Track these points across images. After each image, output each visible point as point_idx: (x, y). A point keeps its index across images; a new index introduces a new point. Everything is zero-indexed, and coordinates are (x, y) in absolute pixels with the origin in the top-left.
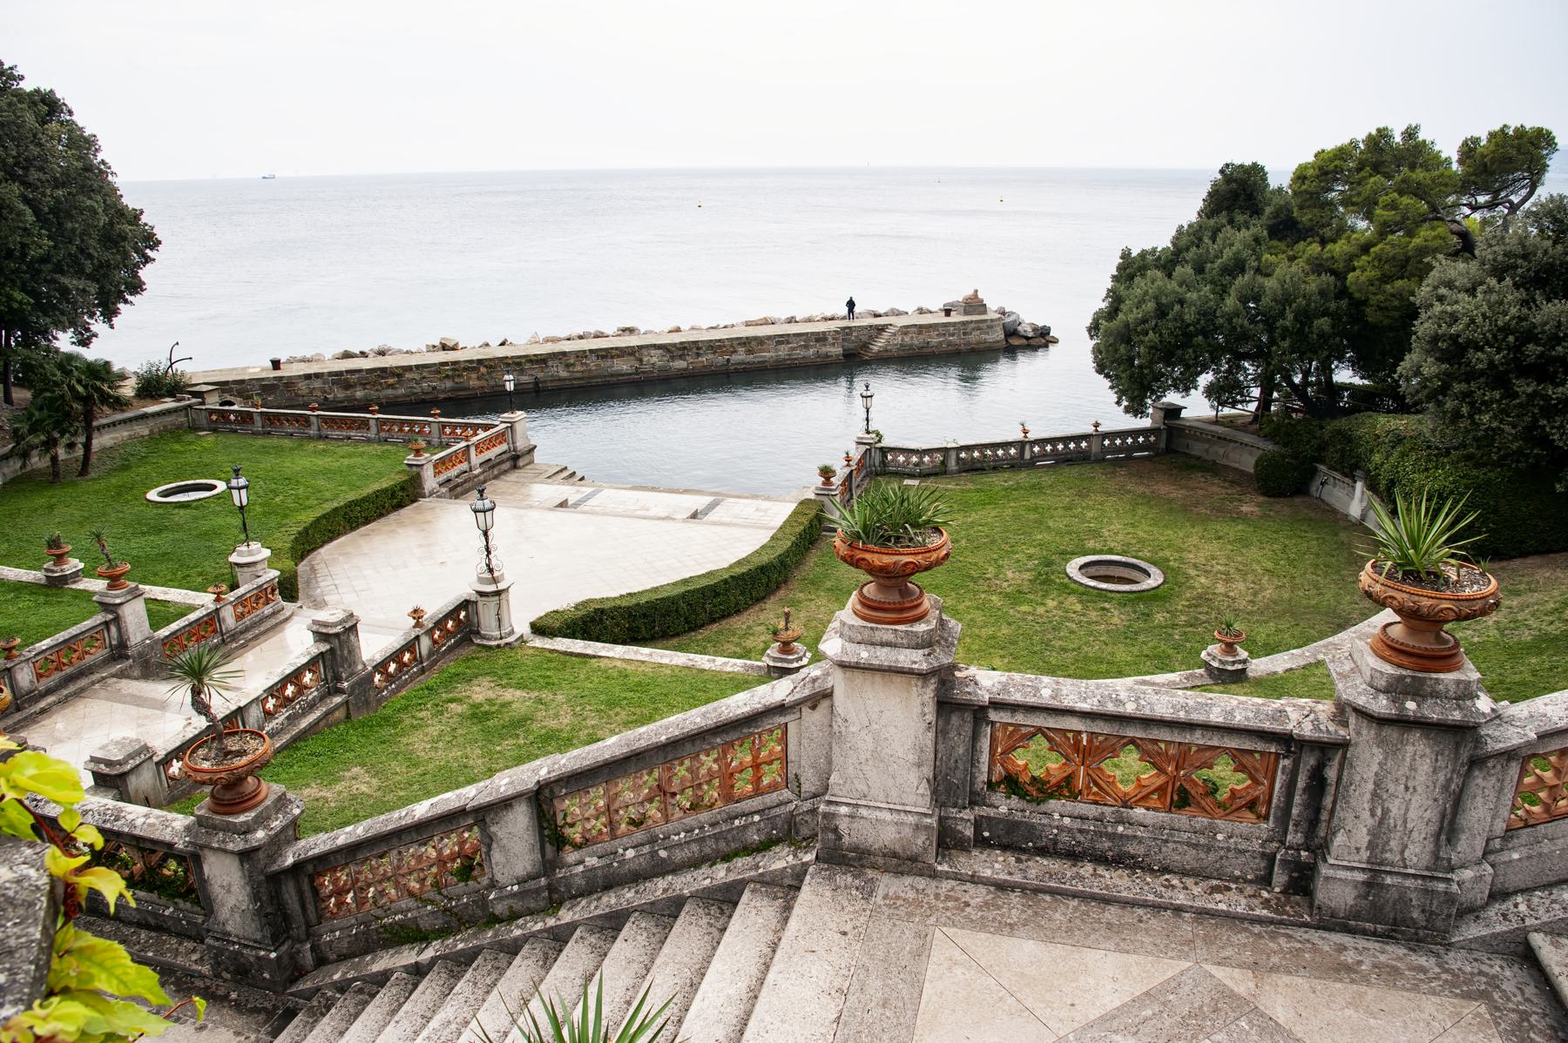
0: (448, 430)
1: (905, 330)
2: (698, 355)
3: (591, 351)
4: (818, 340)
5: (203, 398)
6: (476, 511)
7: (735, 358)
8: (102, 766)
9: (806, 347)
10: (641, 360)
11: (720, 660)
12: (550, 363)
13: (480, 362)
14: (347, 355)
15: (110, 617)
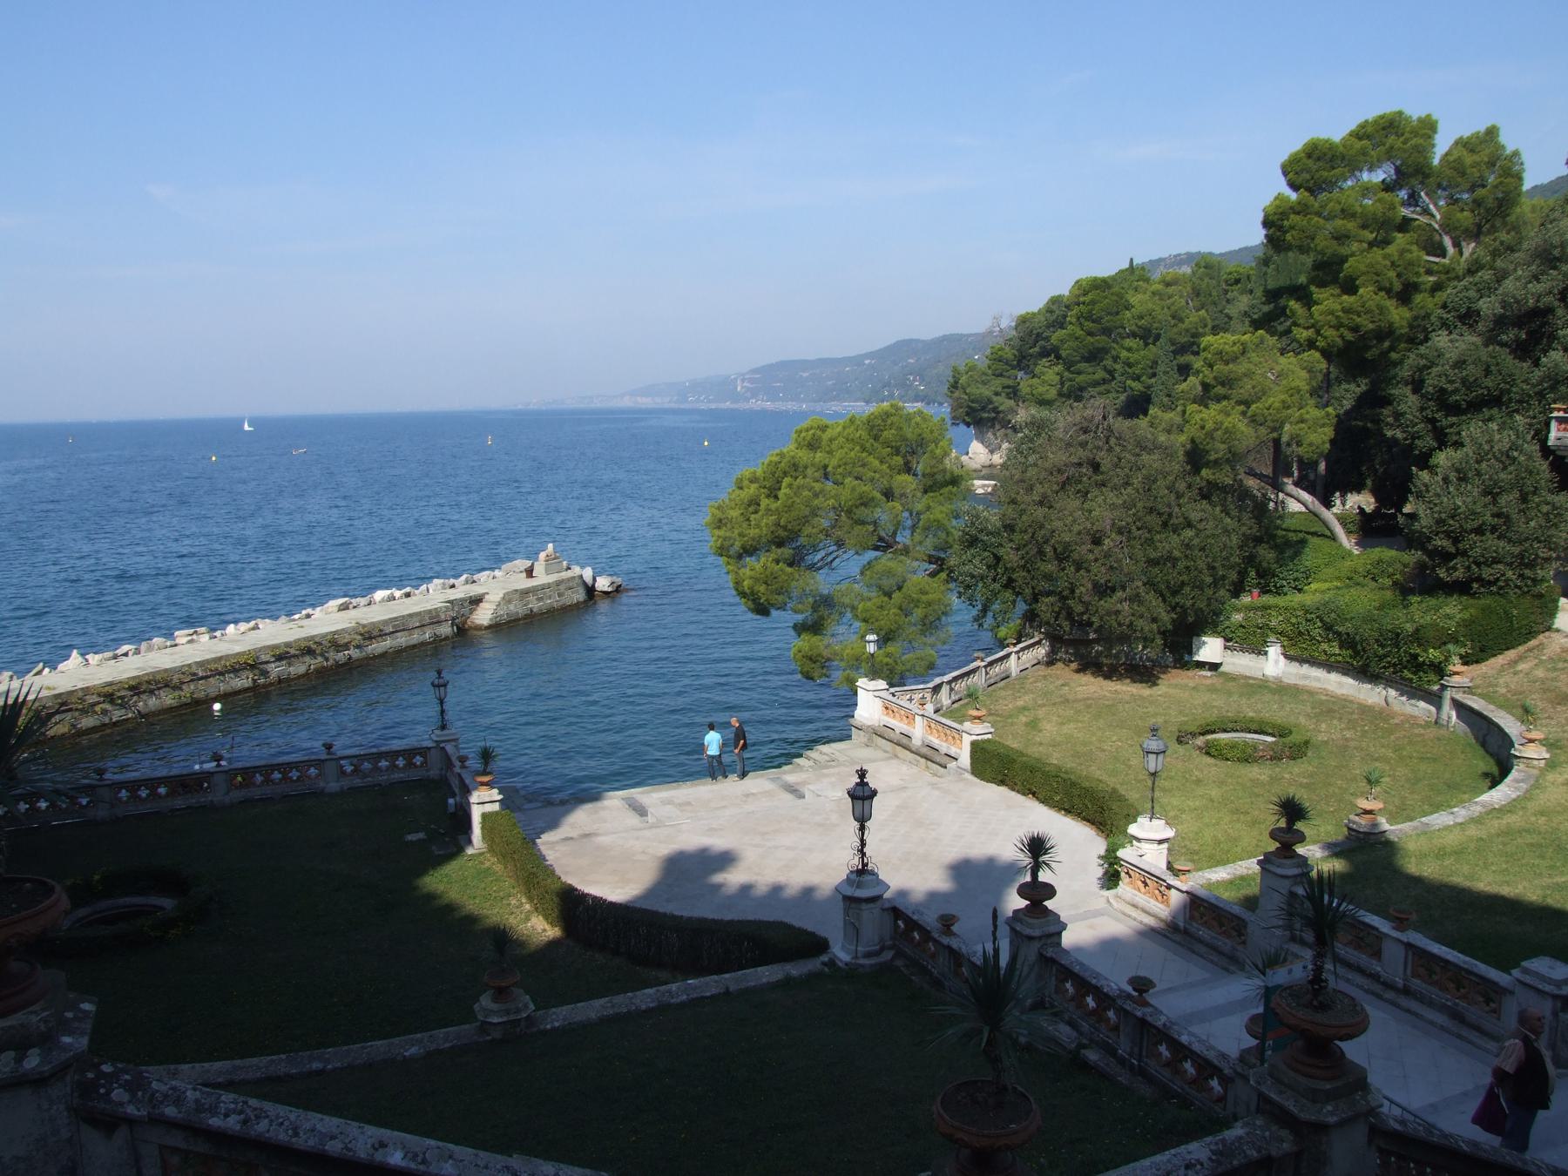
1: (507, 599)
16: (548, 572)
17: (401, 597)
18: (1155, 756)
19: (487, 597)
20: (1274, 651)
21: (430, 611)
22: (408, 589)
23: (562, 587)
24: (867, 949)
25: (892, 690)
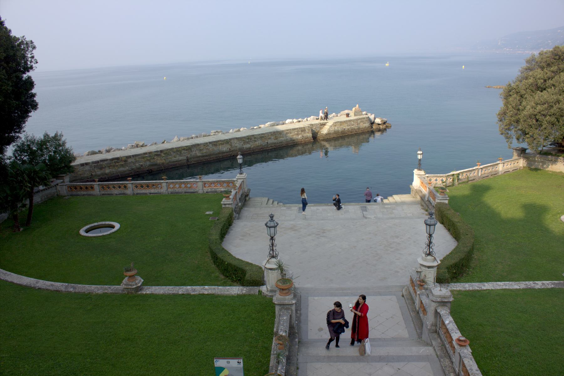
0: (207, 185)
1: (335, 124)
2: (255, 141)
3: (210, 143)
4: (302, 131)
5: (63, 179)
7: (270, 141)
9: (298, 134)
10: (231, 145)
12: (193, 150)
13: (161, 151)
14: (93, 153)
16: (355, 115)
17: (296, 122)
18: (429, 226)
19: (327, 123)
21: (302, 128)
22: (300, 120)
23: (359, 121)
24: (272, 289)
25: (427, 175)
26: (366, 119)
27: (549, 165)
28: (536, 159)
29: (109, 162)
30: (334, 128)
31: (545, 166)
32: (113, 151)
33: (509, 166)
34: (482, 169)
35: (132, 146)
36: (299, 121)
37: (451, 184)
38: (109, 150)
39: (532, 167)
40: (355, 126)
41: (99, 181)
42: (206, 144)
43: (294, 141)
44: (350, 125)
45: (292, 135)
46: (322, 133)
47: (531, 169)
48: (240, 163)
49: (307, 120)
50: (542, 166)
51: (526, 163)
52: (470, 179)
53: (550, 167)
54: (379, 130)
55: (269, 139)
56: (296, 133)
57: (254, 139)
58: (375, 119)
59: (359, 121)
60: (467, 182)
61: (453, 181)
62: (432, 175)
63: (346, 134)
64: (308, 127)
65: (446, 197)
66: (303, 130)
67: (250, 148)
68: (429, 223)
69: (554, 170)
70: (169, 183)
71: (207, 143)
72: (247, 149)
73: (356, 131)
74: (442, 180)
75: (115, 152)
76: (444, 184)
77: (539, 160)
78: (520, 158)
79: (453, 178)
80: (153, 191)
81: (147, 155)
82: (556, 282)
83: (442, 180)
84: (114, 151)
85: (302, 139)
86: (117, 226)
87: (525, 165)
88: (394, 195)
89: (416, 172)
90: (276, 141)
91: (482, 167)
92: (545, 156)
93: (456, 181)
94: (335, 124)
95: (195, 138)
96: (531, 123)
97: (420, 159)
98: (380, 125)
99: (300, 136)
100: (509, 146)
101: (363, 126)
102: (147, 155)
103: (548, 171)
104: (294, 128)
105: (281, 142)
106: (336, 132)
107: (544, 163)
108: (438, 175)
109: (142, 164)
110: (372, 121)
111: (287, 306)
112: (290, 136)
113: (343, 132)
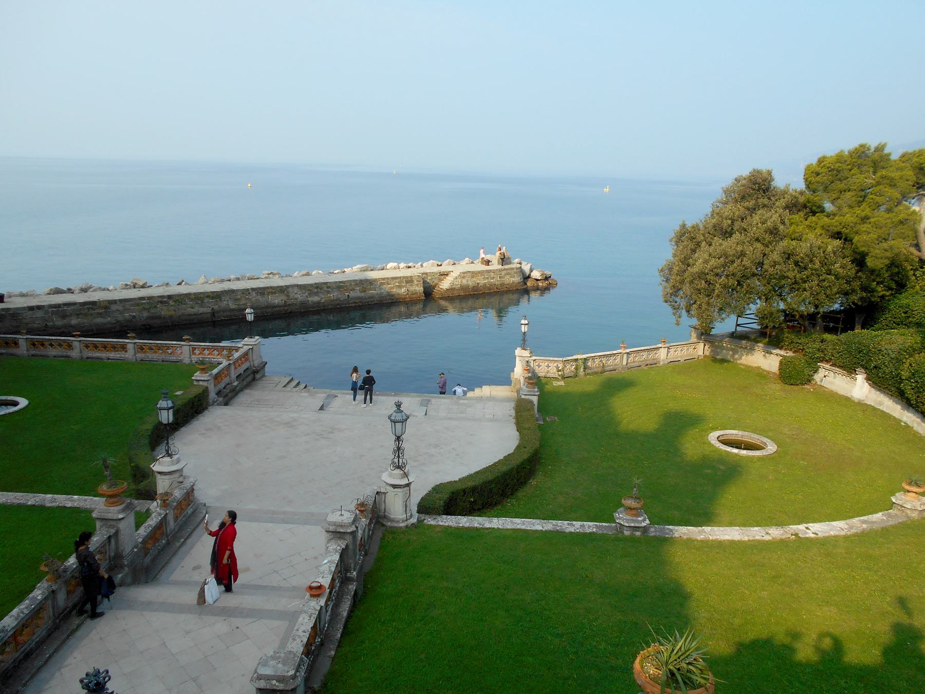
0: (197, 352)
1: (463, 275)
2: (329, 292)
3: (253, 289)
4: (407, 282)
6: (395, 422)
7: (352, 294)
8: (274, 682)
9: (400, 287)
10: (288, 296)
11: (577, 524)
12: (223, 298)
13: (170, 297)
14: (58, 291)
15: (113, 531)
17: (403, 268)
20: (861, 378)
21: (407, 277)
23: (503, 273)
26: (515, 270)
27: (742, 355)
28: (724, 345)
29: (78, 306)
30: (462, 281)
31: (736, 356)
32: (92, 292)
33: (679, 353)
34: (628, 353)
35: (127, 285)
36: (409, 267)
37: (572, 374)
38: (86, 289)
39: (718, 357)
40: (496, 280)
41: (27, 333)
42: (246, 291)
43: (393, 298)
44: (488, 278)
45: (390, 287)
46: (441, 287)
47: (715, 360)
48: (250, 320)
49: (422, 266)
50: (733, 356)
51: (709, 350)
52: (607, 369)
53: (743, 358)
54: (537, 289)
55: (351, 290)
56: (397, 284)
57: (326, 289)
58: (531, 271)
59: (503, 273)
60: (602, 373)
61: (576, 369)
62: (543, 358)
63: (480, 291)
64: (418, 276)
65: (535, 392)
66: (409, 280)
67: (319, 303)
68: (393, 418)
69: (749, 364)
70: (138, 344)
71: (248, 290)
72: (314, 303)
73: (497, 288)
74: (557, 367)
75: (94, 293)
76: (560, 373)
77: (729, 346)
78: (699, 341)
79: (577, 365)
80: (112, 355)
81: (145, 301)
82: (604, 524)
83: (557, 367)
84: (95, 291)
85: (408, 294)
86: (23, 402)
87: (707, 353)
88: (484, 385)
89: (518, 352)
90: (363, 294)
91: (628, 351)
92: (737, 340)
93: (582, 370)
94: (462, 275)
95: (233, 280)
96: (699, 287)
97: (525, 333)
98: (538, 282)
99: (403, 290)
100: (677, 321)
101: (510, 280)
102: (145, 301)
103: (741, 364)
104: (394, 276)
105: (373, 297)
106: (463, 288)
107: (735, 352)
108: (551, 359)
109: (135, 314)
110: (526, 275)
111: (112, 523)
112: (386, 288)
113: (476, 288)
